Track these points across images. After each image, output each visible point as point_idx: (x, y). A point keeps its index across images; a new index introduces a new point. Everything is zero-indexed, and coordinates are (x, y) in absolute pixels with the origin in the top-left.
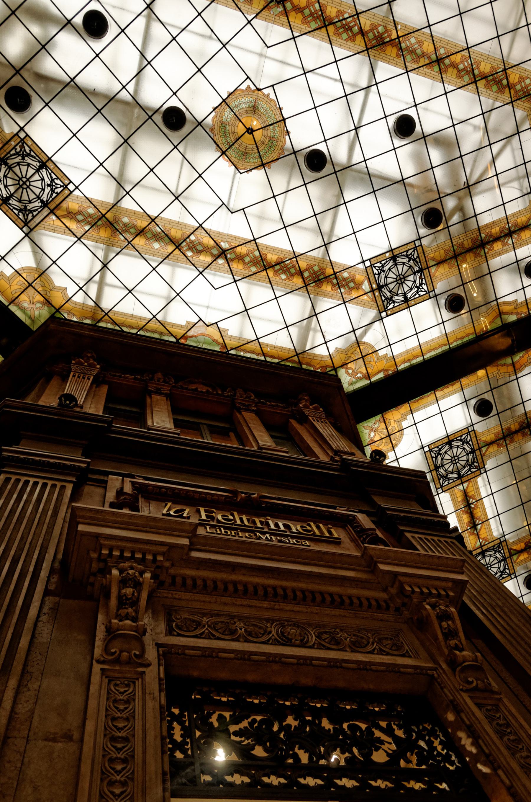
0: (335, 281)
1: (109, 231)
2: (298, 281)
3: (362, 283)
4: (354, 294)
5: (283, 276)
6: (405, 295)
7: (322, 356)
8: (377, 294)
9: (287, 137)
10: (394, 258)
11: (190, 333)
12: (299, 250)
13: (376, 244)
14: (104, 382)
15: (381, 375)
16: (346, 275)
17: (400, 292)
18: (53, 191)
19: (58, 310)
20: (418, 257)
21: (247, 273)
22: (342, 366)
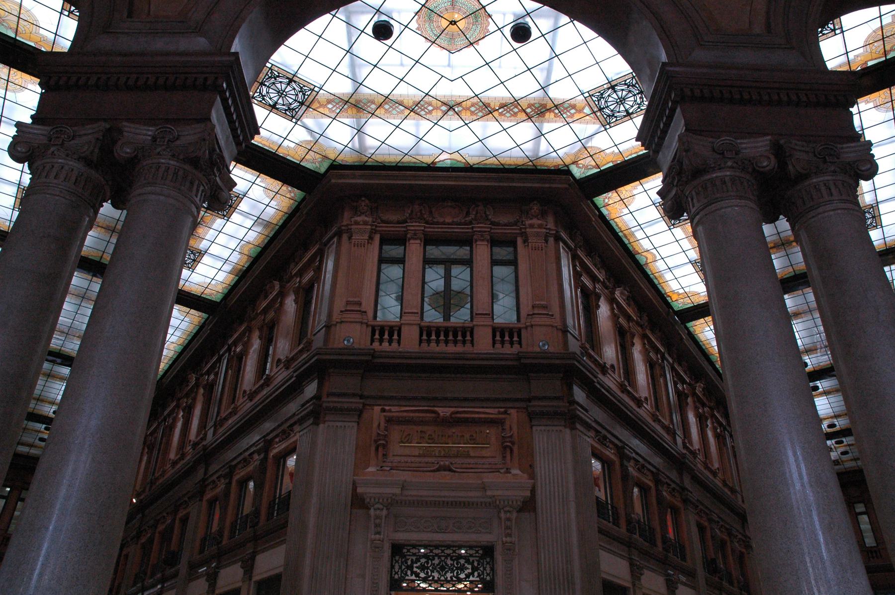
0: (557, 111)
1: (355, 111)
2: (523, 116)
3: (583, 108)
4: (577, 117)
5: (508, 115)
6: (627, 111)
7: (554, 158)
8: (598, 114)
9: (490, 20)
10: (613, 87)
11: (437, 160)
12: (518, 94)
13: (593, 80)
14: (376, 232)
15: (611, 164)
16: (566, 105)
17: (622, 108)
18: (304, 94)
19: (334, 161)
20: (637, 83)
21: (475, 117)
22: (573, 163)
